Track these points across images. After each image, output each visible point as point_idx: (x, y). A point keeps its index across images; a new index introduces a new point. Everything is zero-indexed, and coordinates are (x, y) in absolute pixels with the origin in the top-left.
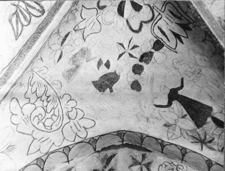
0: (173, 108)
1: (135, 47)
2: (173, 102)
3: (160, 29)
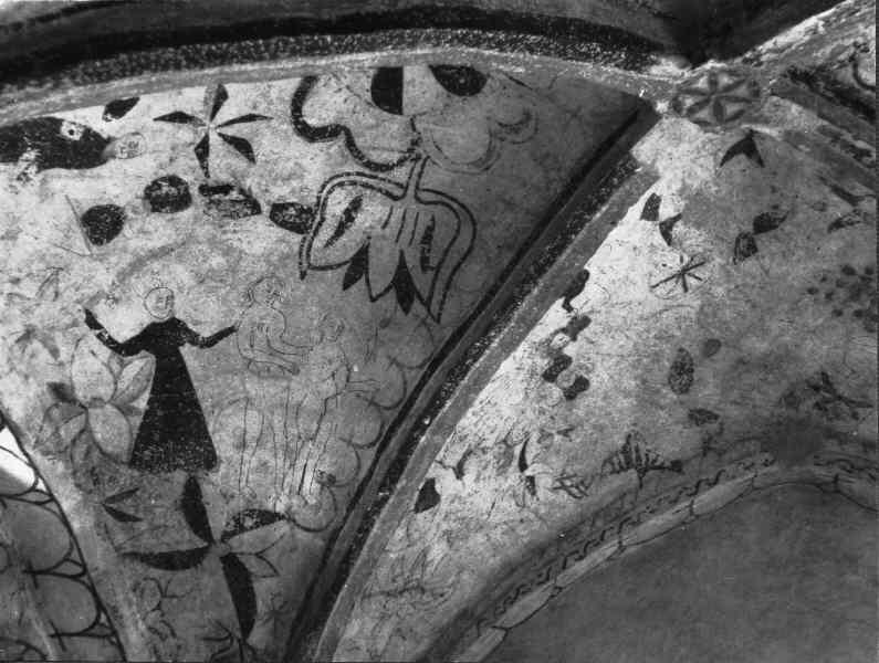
0: (123, 365)
1: (243, 147)
2: (143, 353)
3: (356, 205)
